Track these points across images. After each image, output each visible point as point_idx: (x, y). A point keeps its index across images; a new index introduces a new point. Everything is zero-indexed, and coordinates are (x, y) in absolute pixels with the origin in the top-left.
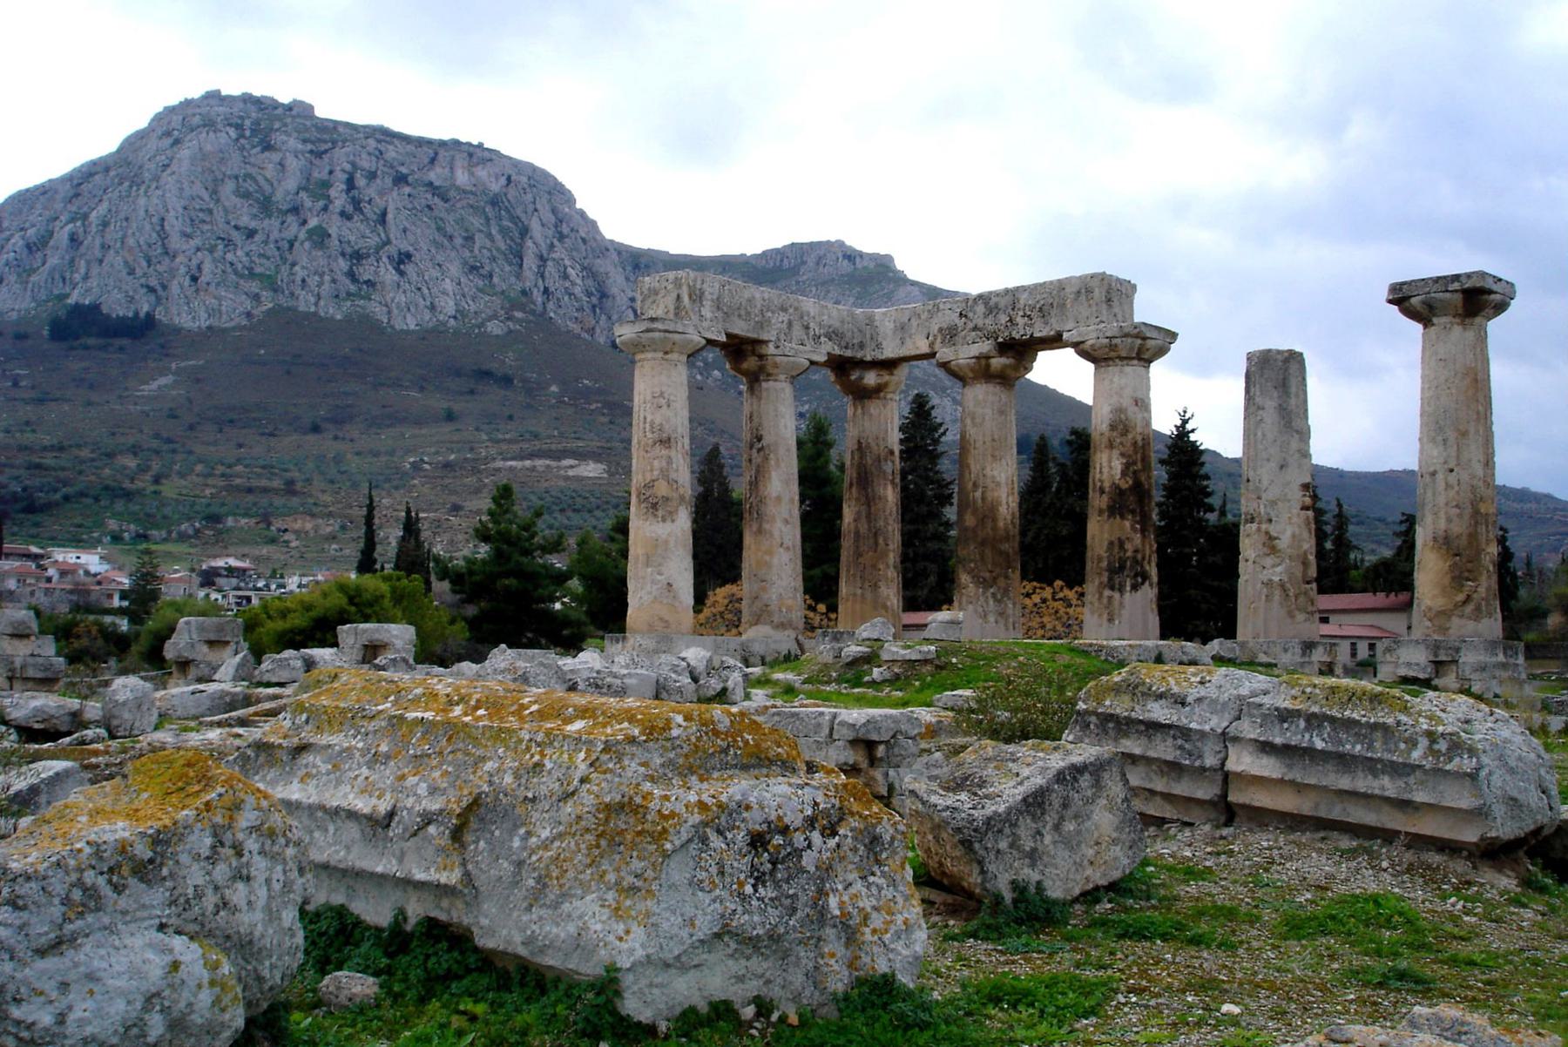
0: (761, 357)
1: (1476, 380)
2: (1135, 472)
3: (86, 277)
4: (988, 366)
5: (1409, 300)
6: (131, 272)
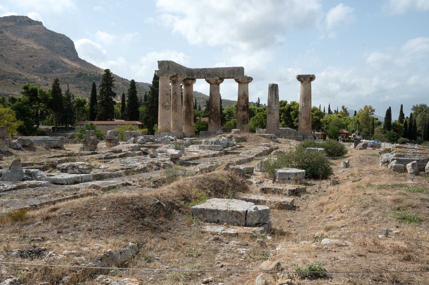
0: (177, 78)
5: (300, 78)
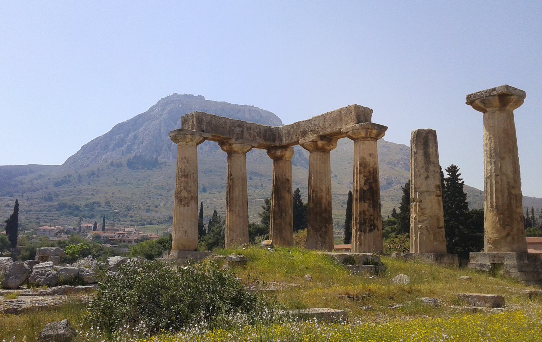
0: (231, 145)
1: (508, 134)
2: (370, 183)
4: (317, 144)
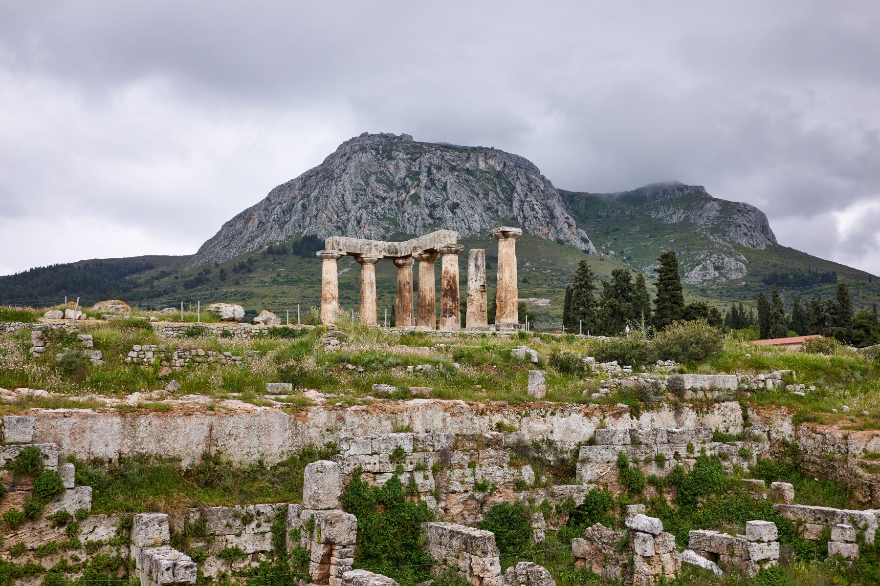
3: (310, 224)
6: (330, 221)
